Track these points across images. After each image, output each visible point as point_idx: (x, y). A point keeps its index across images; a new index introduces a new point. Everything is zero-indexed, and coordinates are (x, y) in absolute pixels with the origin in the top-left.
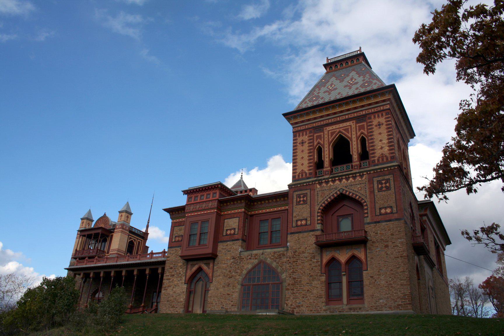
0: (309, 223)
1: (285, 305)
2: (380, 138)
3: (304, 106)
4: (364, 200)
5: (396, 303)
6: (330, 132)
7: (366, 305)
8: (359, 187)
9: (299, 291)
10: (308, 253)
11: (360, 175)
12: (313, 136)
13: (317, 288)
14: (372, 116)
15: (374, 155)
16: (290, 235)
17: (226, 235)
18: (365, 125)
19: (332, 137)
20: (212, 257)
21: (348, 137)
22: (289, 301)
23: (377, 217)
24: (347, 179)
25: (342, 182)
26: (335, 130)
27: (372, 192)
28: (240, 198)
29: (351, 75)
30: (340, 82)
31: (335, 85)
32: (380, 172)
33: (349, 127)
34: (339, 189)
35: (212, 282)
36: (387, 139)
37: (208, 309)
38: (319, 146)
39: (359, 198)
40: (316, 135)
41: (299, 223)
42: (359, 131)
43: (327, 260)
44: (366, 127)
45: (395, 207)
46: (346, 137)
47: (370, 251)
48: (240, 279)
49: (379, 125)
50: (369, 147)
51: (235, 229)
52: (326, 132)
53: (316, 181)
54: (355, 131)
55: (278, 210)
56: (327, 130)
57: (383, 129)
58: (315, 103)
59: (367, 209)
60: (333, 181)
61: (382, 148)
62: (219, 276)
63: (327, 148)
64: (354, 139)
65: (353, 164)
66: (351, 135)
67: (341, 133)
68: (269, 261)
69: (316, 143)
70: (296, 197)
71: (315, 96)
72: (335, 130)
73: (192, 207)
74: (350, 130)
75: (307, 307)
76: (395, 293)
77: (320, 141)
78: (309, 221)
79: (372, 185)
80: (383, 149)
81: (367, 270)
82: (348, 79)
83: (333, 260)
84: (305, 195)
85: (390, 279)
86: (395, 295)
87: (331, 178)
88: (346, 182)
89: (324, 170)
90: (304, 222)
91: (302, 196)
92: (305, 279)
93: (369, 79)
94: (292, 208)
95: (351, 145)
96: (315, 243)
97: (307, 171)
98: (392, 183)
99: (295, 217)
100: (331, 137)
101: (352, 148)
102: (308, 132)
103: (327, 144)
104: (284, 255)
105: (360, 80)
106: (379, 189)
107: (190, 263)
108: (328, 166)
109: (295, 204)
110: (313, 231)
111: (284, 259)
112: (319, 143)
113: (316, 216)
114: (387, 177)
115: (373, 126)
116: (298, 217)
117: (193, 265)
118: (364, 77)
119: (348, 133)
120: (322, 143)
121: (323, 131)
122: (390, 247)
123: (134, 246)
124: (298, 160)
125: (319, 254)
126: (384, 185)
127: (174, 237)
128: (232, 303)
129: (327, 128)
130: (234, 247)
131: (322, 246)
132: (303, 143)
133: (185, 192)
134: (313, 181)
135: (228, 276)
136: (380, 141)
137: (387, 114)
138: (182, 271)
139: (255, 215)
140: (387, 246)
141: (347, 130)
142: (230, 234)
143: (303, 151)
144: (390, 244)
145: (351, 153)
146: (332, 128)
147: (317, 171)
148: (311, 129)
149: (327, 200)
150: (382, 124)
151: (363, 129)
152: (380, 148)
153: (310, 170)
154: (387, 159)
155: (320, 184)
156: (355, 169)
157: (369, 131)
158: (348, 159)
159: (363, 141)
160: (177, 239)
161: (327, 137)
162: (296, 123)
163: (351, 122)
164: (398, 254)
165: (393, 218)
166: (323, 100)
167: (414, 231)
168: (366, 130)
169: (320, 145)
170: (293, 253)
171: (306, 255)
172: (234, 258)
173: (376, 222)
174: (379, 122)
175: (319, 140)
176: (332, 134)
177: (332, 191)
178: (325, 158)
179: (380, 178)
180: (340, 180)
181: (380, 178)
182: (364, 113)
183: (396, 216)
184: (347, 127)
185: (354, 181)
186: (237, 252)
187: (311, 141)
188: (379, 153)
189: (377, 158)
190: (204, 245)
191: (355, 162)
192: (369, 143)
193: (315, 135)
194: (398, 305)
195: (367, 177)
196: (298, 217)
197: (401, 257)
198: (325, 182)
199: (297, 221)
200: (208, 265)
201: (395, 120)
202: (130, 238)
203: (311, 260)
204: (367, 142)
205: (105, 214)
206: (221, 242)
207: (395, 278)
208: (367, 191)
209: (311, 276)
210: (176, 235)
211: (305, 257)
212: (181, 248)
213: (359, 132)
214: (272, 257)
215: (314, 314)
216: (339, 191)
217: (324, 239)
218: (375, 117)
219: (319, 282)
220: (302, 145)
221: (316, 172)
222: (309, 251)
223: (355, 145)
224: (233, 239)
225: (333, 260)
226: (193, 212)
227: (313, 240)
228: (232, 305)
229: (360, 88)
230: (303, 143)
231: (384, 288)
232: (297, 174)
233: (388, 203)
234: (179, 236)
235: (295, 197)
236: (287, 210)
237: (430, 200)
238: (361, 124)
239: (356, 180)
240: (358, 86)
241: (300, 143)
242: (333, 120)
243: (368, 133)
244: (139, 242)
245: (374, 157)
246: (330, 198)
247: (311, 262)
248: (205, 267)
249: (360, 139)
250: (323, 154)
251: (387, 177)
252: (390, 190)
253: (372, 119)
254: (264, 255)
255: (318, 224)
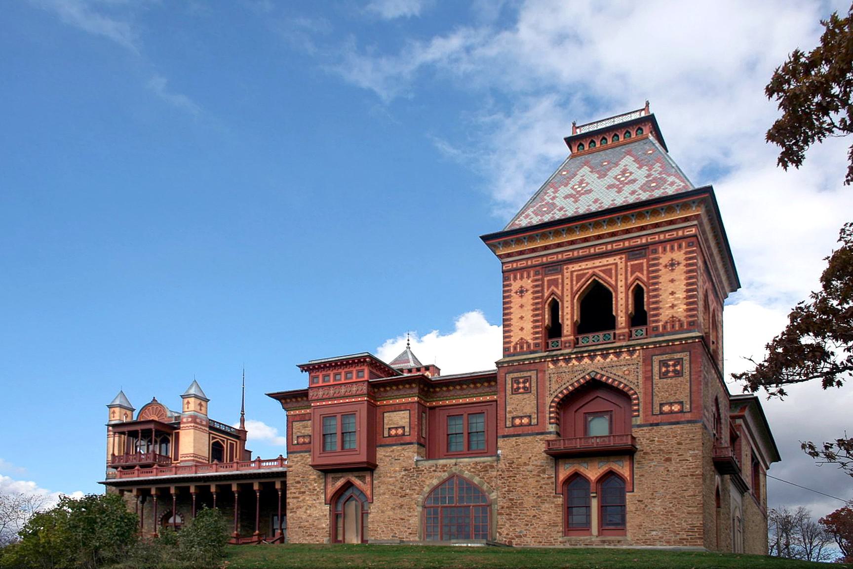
0: (534, 421)
1: (498, 534)
2: (671, 287)
3: (524, 222)
4: (633, 390)
5: (678, 537)
6: (575, 273)
7: (629, 537)
8: (625, 369)
9: (519, 516)
10: (533, 465)
11: (629, 351)
12: (542, 280)
13: (549, 512)
14: (660, 248)
15: (656, 318)
16: (502, 439)
17: (390, 436)
18: (645, 265)
19: (579, 284)
20: (369, 468)
21: (611, 285)
22: (503, 529)
23: (655, 416)
24: (605, 356)
25: (596, 361)
26: (586, 271)
27: (649, 378)
28: (409, 381)
29: (623, 163)
30: (599, 178)
31: (588, 184)
32: (668, 347)
33: (613, 267)
34: (589, 371)
35: (372, 502)
36: (685, 291)
37: (371, 539)
38: (553, 298)
39: (624, 388)
40: (548, 278)
41: (517, 421)
42: (632, 275)
43: (565, 475)
44: (645, 268)
45: (689, 402)
46: (605, 284)
47: (639, 466)
48: (420, 498)
49: (672, 264)
50: (648, 304)
51: (404, 427)
52: (567, 275)
53: (547, 356)
54: (624, 274)
55: (479, 401)
56: (569, 270)
57: (680, 274)
58: (547, 218)
59: (638, 405)
61: (673, 306)
62: (384, 494)
63: (570, 302)
64: (621, 289)
65: (617, 332)
66: (616, 280)
67: (597, 276)
68: (467, 474)
69: (548, 293)
70: (510, 382)
71: (546, 203)
72: (586, 271)
73: (321, 393)
74: (613, 271)
75: (533, 537)
76: (677, 524)
77: (555, 289)
78: (534, 418)
79: (649, 368)
80: (676, 308)
81: (633, 491)
82: (616, 171)
83: (576, 476)
84: (527, 380)
85: (671, 505)
86: (677, 526)
87: (575, 353)
88: (602, 360)
89: (563, 339)
90: (525, 421)
91: (521, 380)
92: (529, 501)
93: (660, 173)
94: (504, 399)
95: (614, 299)
96: (545, 451)
97: (530, 341)
98: (686, 365)
99: (510, 412)
100: (577, 283)
101: (617, 305)
102: (532, 273)
103: (570, 296)
104: (492, 467)
105: (640, 175)
106: (662, 374)
107: (330, 477)
108: (569, 333)
109: (509, 392)
110: (542, 434)
111: (493, 473)
112: (553, 293)
113: (548, 412)
114: (678, 356)
115: (660, 267)
116: (514, 413)
117: (336, 479)
118: (650, 170)
119: (611, 278)
120: (559, 293)
121: (561, 272)
122: (673, 462)
123: (224, 450)
124: (512, 322)
125: (552, 467)
126: (671, 369)
127: (295, 437)
128: (410, 531)
129: (570, 266)
130: (406, 454)
131: (557, 457)
132: (522, 292)
133: (305, 368)
134: (541, 358)
135: (400, 495)
136: (670, 294)
137: (689, 246)
138: (318, 486)
139: (438, 407)
140: (668, 460)
141: (608, 272)
142: (396, 435)
143: (522, 306)
144: (674, 456)
145: (614, 313)
146: (580, 266)
147: (550, 341)
148: (538, 268)
149: (567, 388)
150: (679, 264)
151: (639, 272)
152: (670, 307)
153: (536, 338)
154: (681, 325)
155: (555, 362)
156: (620, 340)
157: (650, 275)
158: (610, 323)
159: (638, 294)
160: (301, 440)
161: (569, 284)
162: (509, 255)
163: (617, 258)
164: (686, 471)
165: (683, 419)
166: (562, 212)
167: (717, 439)
168: (645, 272)
169: (555, 297)
170: (507, 465)
171: (530, 468)
172: (406, 470)
173: (651, 425)
174: (672, 260)
175: (553, 287)
176: (579, 278)
177: (576, 374)
178: (565, 320)
179: (664, 357)
180: (592, 358)
181: (664, 356)
182: (644, 241)
183: (688, 416)
184: (609, 267)
185: (616, 359)
186: (410, 461)
187: (538, 290)
188: (668, 315)
189: (663, 323)
190: (350, 450)
191: (620, 328)
192: (649, 297)
193: (546, 279)
194: (680, 539)
195: (641, 355)
196: (514, 413)
197: (692, 475)
198: (565, 359)
199: (513, 418)
200: (362, 478)
201: (704, 257)
202: (214, 438)
203: (539, 476)
204: (645, 296)
205: (154, 400)
206: (381, 446)
207: (678, 503)
208: (640, 378)
209: (539, 497)
210: (299, 434)
211: (528, 471)
212: (312, 453)
213: (631, 277)
214: (472, 470)
215: (544, 547)
216: (588, 374)
217: (561, 446)
218: (665, 250)
219: (553, 506)
220: (522, 296)
221: (548, 343)
222: (535, 463)
223: (622, 299)
224: (402, 442)
225: (576, 476)
226: (323, 400)
227: (543, 447)
228: (410, 534)
229: (640, 192)
230: (522, 292)
231: (661, 516)
232: (513, 344)
233: (677, 397)
234: (304, 437)
235: (509, 381)
236: (496, 401)
237: (753, 395)
238: (636, 262)
239: (620, 358)
240: (636, 186)
241: (516, 293)
242: (581, 253)
243: (649, 278)
244: (232, 445)
245: (657, 321)
246: (572, 385)
247: (539, 478)
248: (357, 482)
249: (634, 288)
250: (560, 313)
251: (678, 356)
252: (682, 376)
253: (658, 254)
254: (457, 467)
255: (550, 423)
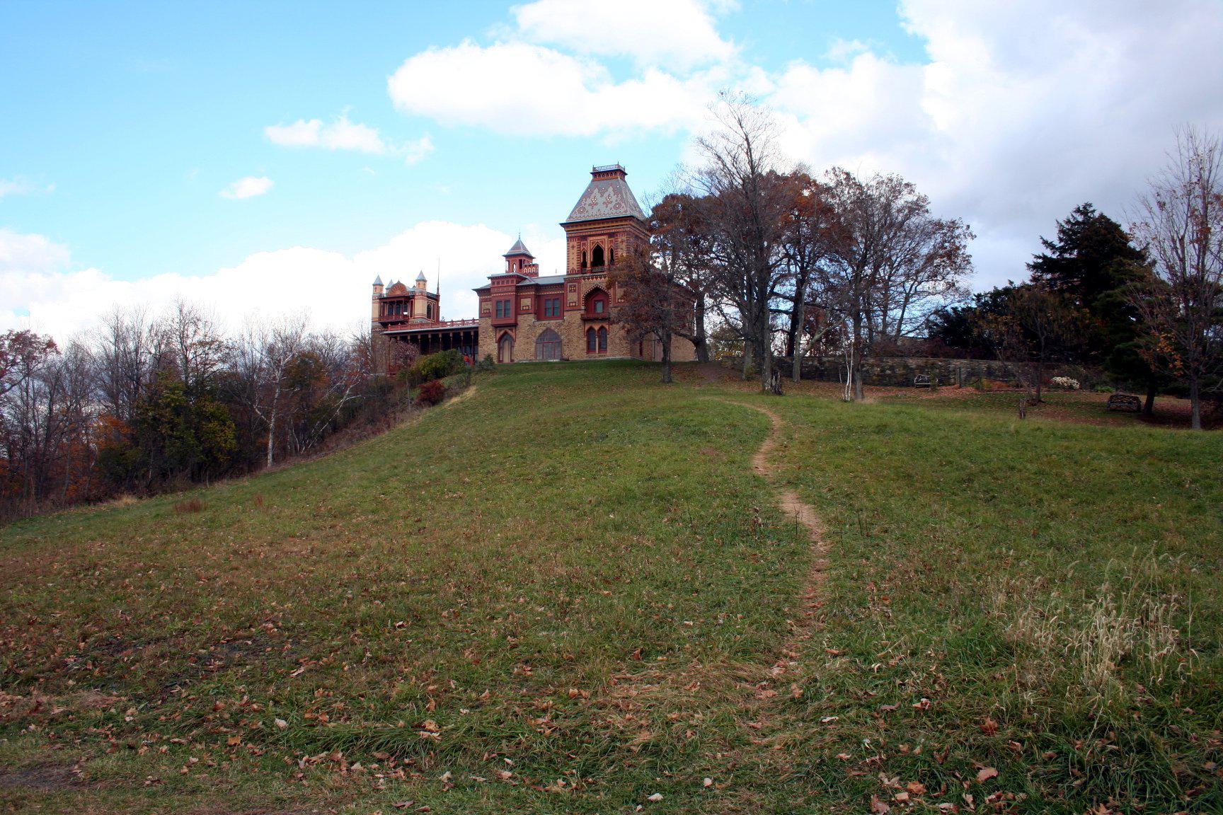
48: (535, 339)
60: (592, 279)
68: (553, 328)
83: (591, 328)
84: (575, 286)
92: (575, 339)
131: (585, 320)
180: (596, 278)
225: (591, 328)
227: (579, 316)
230: (573, 247)
